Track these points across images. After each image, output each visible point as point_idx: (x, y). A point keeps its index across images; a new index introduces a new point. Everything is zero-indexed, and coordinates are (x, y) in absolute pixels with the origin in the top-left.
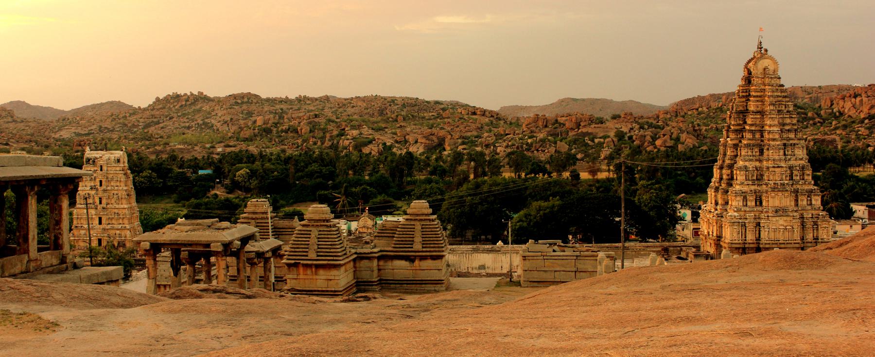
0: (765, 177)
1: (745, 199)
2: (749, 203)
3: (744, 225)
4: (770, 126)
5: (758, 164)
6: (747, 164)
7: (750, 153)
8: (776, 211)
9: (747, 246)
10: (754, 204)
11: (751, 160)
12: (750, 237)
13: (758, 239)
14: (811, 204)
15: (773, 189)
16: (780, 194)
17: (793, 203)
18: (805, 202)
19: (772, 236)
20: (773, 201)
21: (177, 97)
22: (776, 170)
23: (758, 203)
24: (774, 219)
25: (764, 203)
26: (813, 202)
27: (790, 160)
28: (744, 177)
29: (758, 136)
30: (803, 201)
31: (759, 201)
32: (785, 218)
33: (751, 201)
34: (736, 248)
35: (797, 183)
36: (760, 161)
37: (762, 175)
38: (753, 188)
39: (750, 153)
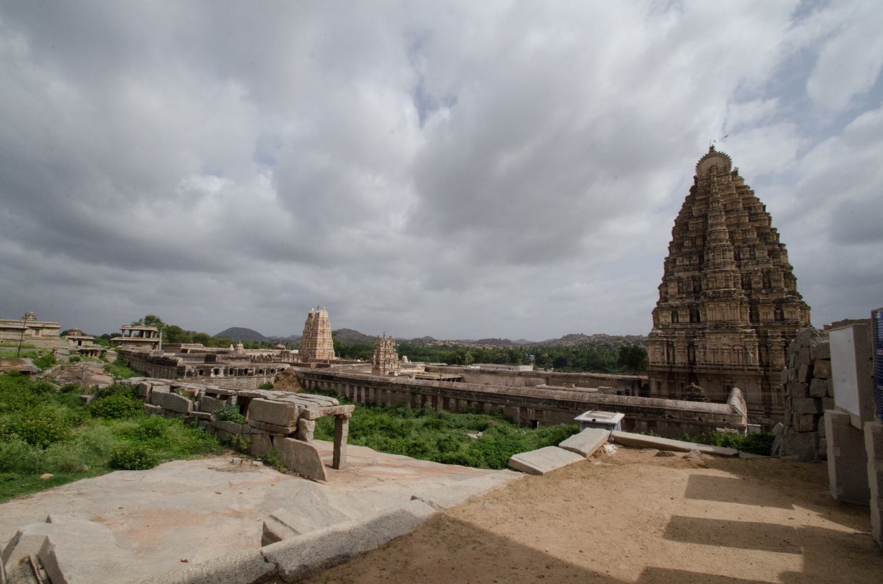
0: (703, 287)
1: (675, 315)
2: (681, 319)
3: (670, 345)
4: (712, 226)
5: (697, 273)
6: (682, 274)
7: (686, 262)
8: (716, 327)
9: (674, 370)
10: (688, 319)
11: (688, 270)
12: (680, 359)
13: (692, 363)
14: (782, 319)
15: (712, 299)
16: (723, 305)
17: (747, 317)
18: (771, 316)
19: (710, 357)
20: (712, 314)
21: (572, 335)
22: (719, 275)
23: (695, 319)
24: (713, 337)
25: (702, 319)
26: (786, 316)
27: (746, 264)
28: (676, 290)
29: (699, 242)
30: (767, 314)
31: (695, 317)
32: (731, 336)
33: (683, 316)
34: (660, 372)
35: (758, 291)
36: (700, 270)
37: (700, 286)
38: (688, 301)
39: (688, 263)
